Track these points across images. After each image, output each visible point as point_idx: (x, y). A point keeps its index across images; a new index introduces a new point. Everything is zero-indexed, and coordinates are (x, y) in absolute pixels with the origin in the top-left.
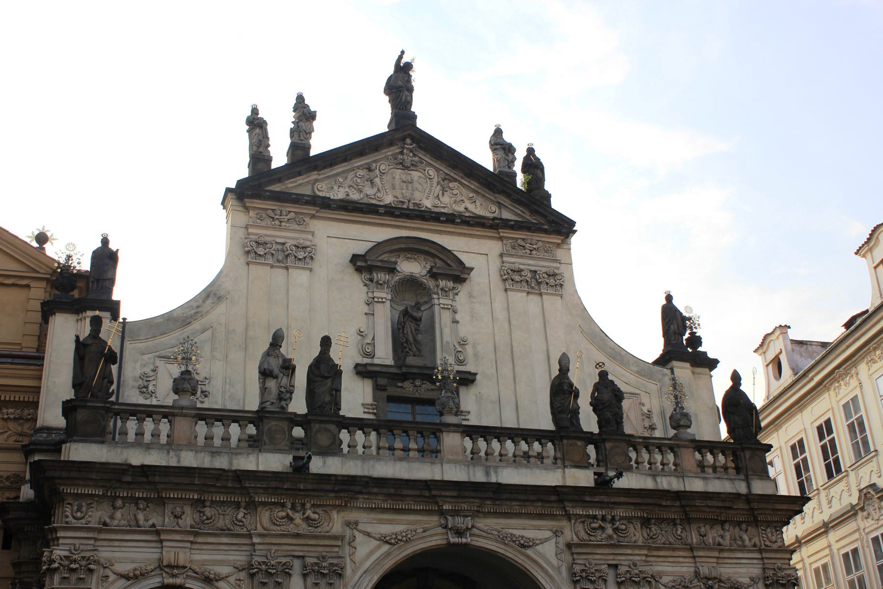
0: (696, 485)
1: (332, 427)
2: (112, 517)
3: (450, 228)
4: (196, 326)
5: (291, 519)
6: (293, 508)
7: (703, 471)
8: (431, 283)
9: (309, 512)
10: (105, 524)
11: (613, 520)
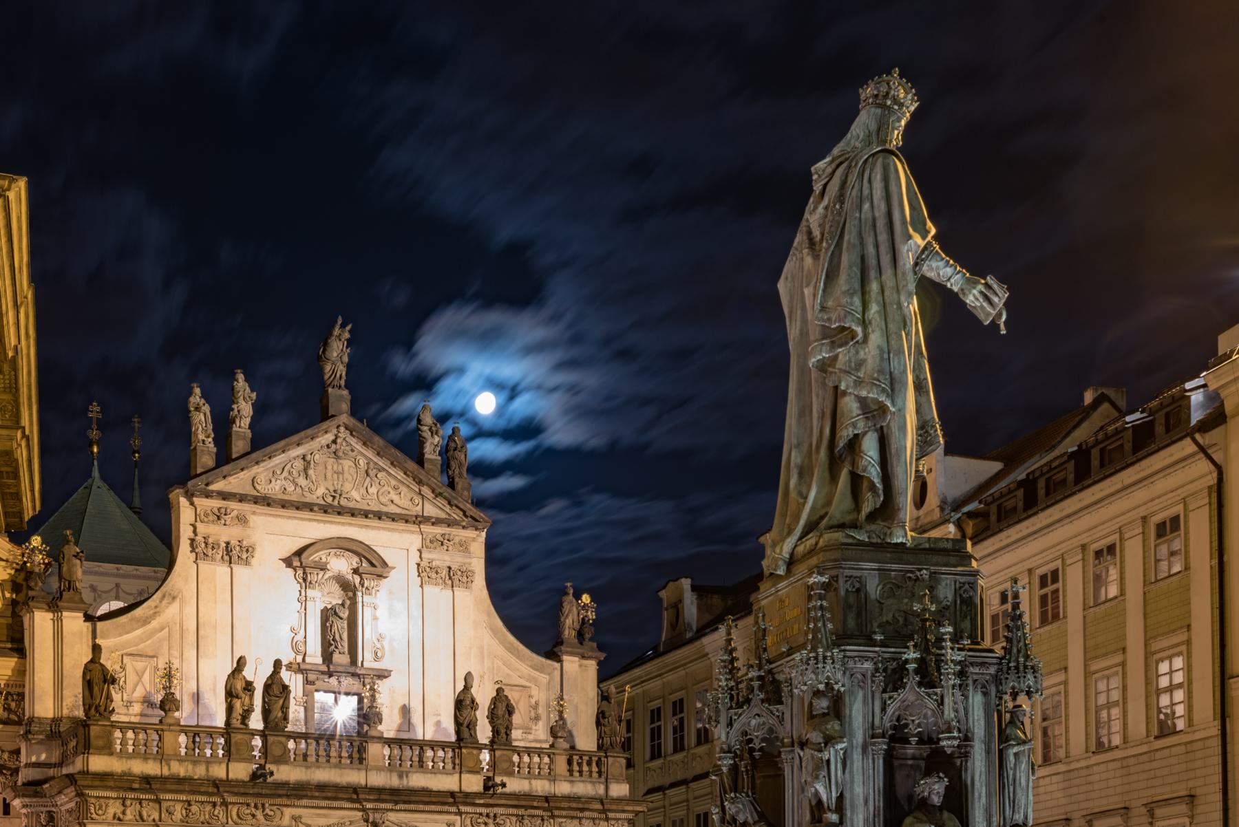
0: (564, 788)
1: (283, 739)
2: (124, 813)
3: (376, 523)
4: (155, 624)
5: (254, 816)
6: (256, 807)
7: (571, 775)
8: (357, 579)
9: (267, 811)
10: (119, 819)
11: (495, 816)
